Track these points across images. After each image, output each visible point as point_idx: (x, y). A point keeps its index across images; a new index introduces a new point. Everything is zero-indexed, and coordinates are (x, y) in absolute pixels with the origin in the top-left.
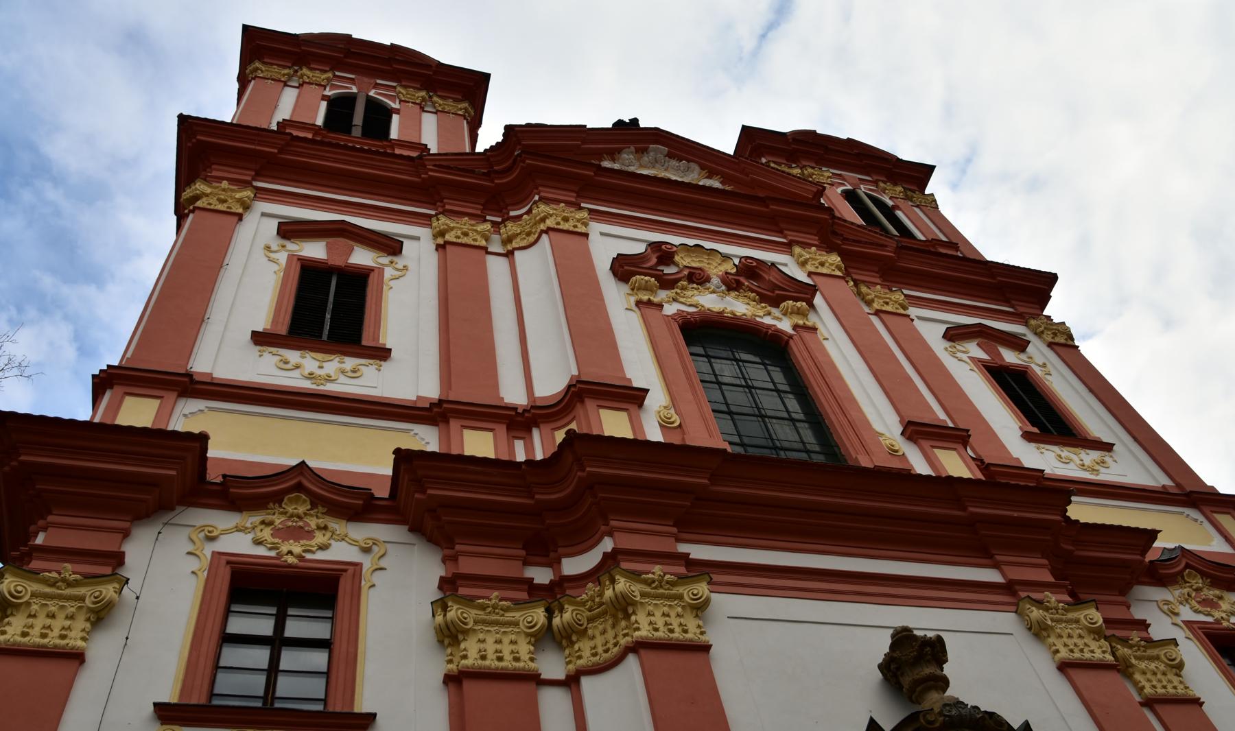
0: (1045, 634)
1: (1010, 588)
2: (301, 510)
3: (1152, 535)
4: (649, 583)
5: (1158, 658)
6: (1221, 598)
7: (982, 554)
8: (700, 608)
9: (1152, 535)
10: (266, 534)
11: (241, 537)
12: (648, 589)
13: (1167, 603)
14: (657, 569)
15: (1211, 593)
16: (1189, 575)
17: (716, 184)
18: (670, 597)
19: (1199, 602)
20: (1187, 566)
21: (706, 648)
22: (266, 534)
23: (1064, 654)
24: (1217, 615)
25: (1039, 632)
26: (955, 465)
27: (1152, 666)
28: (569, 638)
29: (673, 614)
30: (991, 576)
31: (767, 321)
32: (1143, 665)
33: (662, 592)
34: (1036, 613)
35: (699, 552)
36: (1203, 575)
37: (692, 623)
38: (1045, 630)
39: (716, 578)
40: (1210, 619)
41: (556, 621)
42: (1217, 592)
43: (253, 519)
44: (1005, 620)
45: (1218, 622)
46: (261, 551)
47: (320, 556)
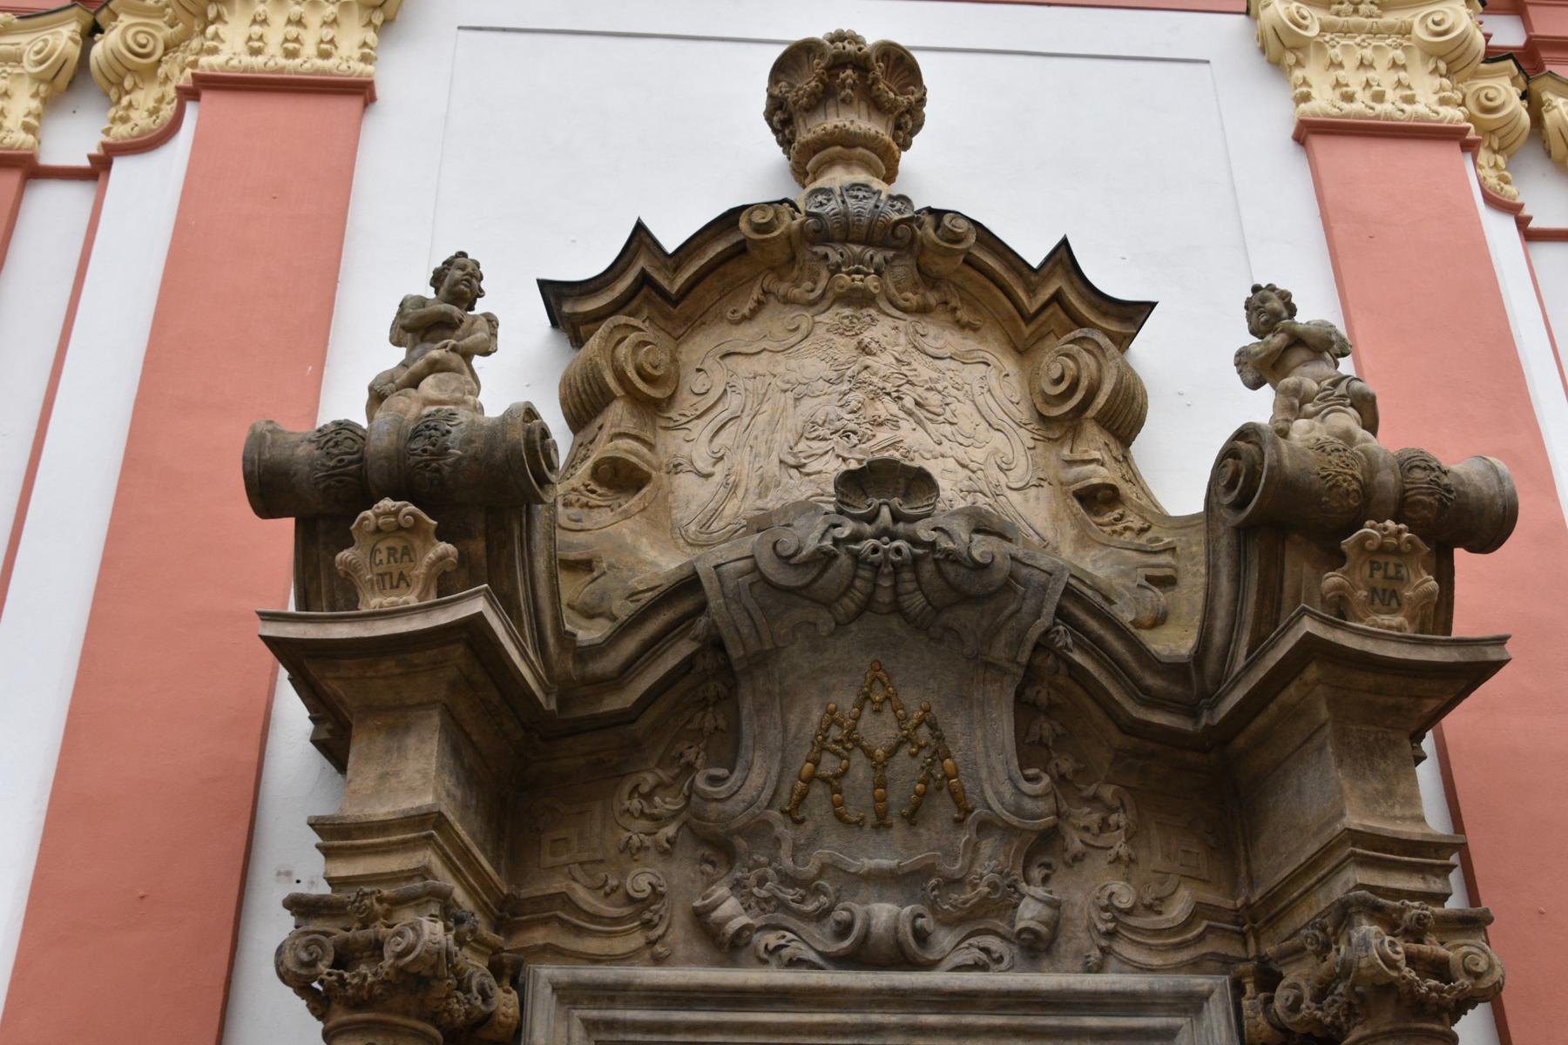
0: (1290, 58)
21: (362, 91)
23: (1324, 103)
25: (1281, 51)
28: (120, 84)
29: (313, 20)
38: (1293, 49)
41: (98, 51)
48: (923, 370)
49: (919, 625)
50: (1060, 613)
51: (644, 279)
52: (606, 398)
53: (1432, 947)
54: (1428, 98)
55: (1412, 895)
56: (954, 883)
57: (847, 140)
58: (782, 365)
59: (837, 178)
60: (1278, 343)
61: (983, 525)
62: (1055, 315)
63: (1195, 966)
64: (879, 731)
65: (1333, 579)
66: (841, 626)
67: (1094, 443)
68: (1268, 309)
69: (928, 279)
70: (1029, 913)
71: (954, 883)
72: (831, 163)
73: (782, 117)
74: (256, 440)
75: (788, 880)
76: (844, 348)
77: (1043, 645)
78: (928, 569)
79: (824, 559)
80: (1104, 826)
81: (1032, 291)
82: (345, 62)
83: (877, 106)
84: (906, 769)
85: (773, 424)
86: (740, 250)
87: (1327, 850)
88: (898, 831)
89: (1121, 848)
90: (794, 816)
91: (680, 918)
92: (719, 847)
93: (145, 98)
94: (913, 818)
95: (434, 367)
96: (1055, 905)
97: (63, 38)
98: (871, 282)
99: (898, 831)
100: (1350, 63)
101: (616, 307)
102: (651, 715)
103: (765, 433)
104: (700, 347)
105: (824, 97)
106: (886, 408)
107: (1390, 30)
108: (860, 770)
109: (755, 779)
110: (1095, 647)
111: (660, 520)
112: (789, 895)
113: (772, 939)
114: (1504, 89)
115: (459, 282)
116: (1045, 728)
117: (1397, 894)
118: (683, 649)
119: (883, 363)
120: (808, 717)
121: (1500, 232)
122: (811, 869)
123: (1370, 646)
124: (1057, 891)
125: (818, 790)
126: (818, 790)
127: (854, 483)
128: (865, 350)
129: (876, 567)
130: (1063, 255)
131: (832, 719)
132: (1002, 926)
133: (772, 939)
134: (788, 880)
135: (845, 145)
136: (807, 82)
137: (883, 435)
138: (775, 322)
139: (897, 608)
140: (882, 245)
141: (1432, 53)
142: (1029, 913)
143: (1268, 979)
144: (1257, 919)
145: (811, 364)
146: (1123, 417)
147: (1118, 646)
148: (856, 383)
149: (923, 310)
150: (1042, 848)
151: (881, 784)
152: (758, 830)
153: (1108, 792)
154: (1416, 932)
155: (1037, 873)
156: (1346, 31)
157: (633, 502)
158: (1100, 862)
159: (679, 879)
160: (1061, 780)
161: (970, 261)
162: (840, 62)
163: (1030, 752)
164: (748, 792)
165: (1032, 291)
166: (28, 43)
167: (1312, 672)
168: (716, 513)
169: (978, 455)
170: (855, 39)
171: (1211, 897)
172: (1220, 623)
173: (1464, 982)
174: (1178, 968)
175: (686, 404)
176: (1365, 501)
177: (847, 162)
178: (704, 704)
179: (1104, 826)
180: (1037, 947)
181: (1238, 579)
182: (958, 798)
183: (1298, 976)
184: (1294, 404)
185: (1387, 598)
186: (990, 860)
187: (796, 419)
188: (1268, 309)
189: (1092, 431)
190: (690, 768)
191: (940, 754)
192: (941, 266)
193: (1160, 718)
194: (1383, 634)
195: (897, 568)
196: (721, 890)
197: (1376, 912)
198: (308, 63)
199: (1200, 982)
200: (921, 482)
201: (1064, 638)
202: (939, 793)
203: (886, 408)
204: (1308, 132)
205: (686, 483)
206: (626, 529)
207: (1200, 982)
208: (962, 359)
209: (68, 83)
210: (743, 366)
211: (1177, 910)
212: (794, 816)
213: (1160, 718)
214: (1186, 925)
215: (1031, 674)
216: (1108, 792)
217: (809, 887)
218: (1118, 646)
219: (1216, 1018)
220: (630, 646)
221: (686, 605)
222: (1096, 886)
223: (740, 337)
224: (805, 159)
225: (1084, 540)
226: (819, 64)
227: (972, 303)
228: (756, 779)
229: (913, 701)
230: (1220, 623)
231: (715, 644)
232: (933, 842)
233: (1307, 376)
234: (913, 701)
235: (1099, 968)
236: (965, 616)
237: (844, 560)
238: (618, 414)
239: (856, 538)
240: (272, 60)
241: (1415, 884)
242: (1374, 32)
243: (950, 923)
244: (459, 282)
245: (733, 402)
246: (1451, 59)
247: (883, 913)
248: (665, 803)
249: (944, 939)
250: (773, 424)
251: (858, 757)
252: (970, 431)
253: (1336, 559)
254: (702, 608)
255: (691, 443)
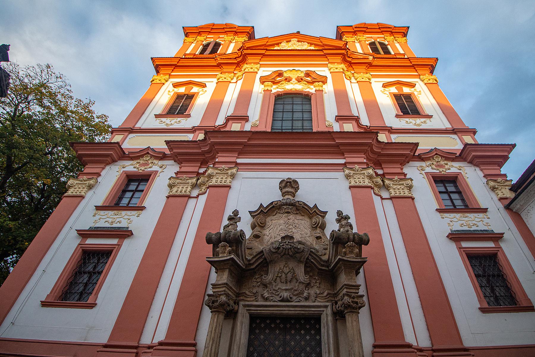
1: (345, 165)
2: (148, 159)
3: (417, 144)
4: (220, 170)
5: (403, 184)
6: (447, 164)
7: (341, 154)
8: (233, 176)
9: (417, 144)
10: (137, 166)
11: (130, 167)
12: (219, 172)
13: (421, 167)
14: (223, 166)
15: (442, 163)
16: (437, 157)
17: (312, 48)
18: (225, 174)
19: (436, 166)
20: (436, 154)
21: (229, 187)
22: (137, 166)
23: (353, 183)
24: (441, 170)
25: (348, 177)
26: (349, 127)
27: (399, 187)
30: (342, 161)
31: (308, 90)
32: (395, 187)
33: (224, 172)
34: (347, 171)
35: (239, 161)
36: (442, 156)
37: (229, 179)
39: (239, 167)
40: (438, 171)
42: (446, 162)
43: (135, 162)
44: (340, 175)
45: (440, 172)
46: (135, 170)
47: (149, 170)
48: (296, 221)
49: (291, 256)
50: (310, 254)
51: (262, 210)
52: (256, 226)
53: (356, 300)
54: (367, 182)
55: (353, 293)
56: (296, 290)
57: (288, 192)
58: (279, 221)
59: (287, 197)
60: (342, 218)
61: (300, 243)
62: (314, 214)
63: (327, 301)
64: (286, 270)
65: (344, 250)
66: (282, 257)
67: (318, 230)
68: (339, 213)
69: (297, 210)
70: (305, 294)
71: (296, 290)
72: (286, 195)
73: (281, 188)
74: (208, 235)
75: (274, 290)
76: (286, 219)
77: (308, 259)
78: (292, 249)
79: (278, 248)
80: (316, 282)
81: (311, 211)
82: (228, 183)
83: (292, 187)
84: (290, 276)
85: (277, 229)
86: (273, 207)
87: (343, 287)
88: (289, 283)
89: (318, 285)
90: (275, 281)
91: (260, 295)
92: (265, 286)
93: (204, 188)
94: (290, 282)
95: (231, 225)
96: (309, 293)
97: (194, 180)
98: (290, 211)
99: (289, 283)
100: (357, 178)
101: (258, 214)
102: (257, 268)
103: (276, 229)
104: (268, 219)
105: (285, 186)
106: (291, 227)
107: (362, 174)
108: (284, 275)
109: (270, 277)
110: (315, 259)
111: (262, 243)
112: (274, 292)
113: (272, 298)
114: (379, 180)
115: (236, 213)
116: (308, 269)
117: (351, 292)
118: (261, 260)
119: (291, 221)
120: (277, 269)
121: (377, 200)
122: (277, 289)
123: (349, 259)
124: (309, 291)
125: (278, 278)
126: (278, 278)
127: (283, 238)
128: (289, 219)
129: (286, 249)
130: (315, 206)
131: (280, 269)
132: (302, 296)
133: (272, 298)
134: (274, 290)
135: (288, 193)
136: (283, 185)
137: (290, 230)
138: (278, 215)
139: (288, 254)
140: (292, 206)
141: (367, 176)
142: (305, 294)
143: (336, 303)
144: (336, 295)
145: (282, 221)
146: (323, 227)
147: (318, 259)
148: (287, 224)
149: (297, 214)
150: (308, 285)
151: (286, 277)
152: (270, 283)
153: (317, 278)
154: (354, 298)
155: (307, 289)
156: (356, 174)
157: (258, 240)
158: (316, 287)
159: (260, 290)
160: (311, 276)
161: (303, 207)
162: (287, 182)
163: (306, 273)
164: (269, 279)
165: (311, 211)
166: (190, 181)
167: (341, 263)
168: (269, 241)
169: (303, 233)
170: (290, 179)
171: (329, 292)
172: (331, 256)
173: (360, 305)
174: (325, 302)
175: (267, 226)
176: (349, 240)
177: (288, 195)
178: (264, 267)
179: (316, 282)
180: (307, 299)
181: (333, 250)
182: (296, 279)
183: (340, 303)
184: (341, 226)
185: (351, 252)
186: (302, 287)
187: (279, 229)
188: (339, 213)
189: (318, 229)
190: (262, 275)
191: (294, 273)
192: (299, 208)
193: (323, 268)
194: (351, 257)
195: (288, 249)
196: (265, 291)
197: (348, 295)
198: (223, 183)
199: (327, 304)
200: (292, 238)
201: (310, 257)
202: (295, 278)
203: (291, 227)
204: (350, 187)
205: (266, 237)
206: (256, 244)
207: (327, 304)
208: (301, 220)
209: (194, 186)
210: (274, 221)
211: (325, 294)
212: (275, 281)
213: (323, 268)
214: (326, 296)
215: (306, 263)
216: (317, 278)
217: (277, 291)
218: (318, 259)
219: (329, 309)
220: (254, 259)
221: (262, 254)
222: (313, 291)
223: (273, 218)
224: (284, 194)
225: (316, 244)
226: (285, 182)
227: (304, 212)
228: (270, 277)
229: (291, 266)
230: (331, 256)
231: (265, 259)
232: (294, 285)
233: (344, 222)
234: (291, 266)
235: (315, 302)
236: (298, 255)
237: (282, 248)
238: (257, 228)
239: (283, 245)
240: (219, 183)
241: (354, 291)
242: (360, 174)
243: (295, 295)
244: (236, 213)
245: (272, 226)
246: (370, 177)
247: (286, 294)
248: (258, 280)
249: (294, 298)
250: (277, 229)
251: (283, 274)
252: (301, 230)
253: (345, 247)
254: (264, 255)
255: (267, 232)
